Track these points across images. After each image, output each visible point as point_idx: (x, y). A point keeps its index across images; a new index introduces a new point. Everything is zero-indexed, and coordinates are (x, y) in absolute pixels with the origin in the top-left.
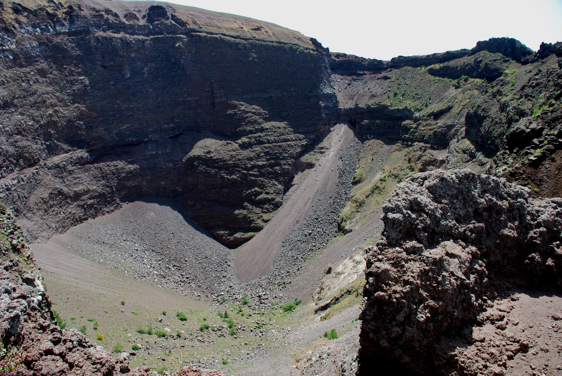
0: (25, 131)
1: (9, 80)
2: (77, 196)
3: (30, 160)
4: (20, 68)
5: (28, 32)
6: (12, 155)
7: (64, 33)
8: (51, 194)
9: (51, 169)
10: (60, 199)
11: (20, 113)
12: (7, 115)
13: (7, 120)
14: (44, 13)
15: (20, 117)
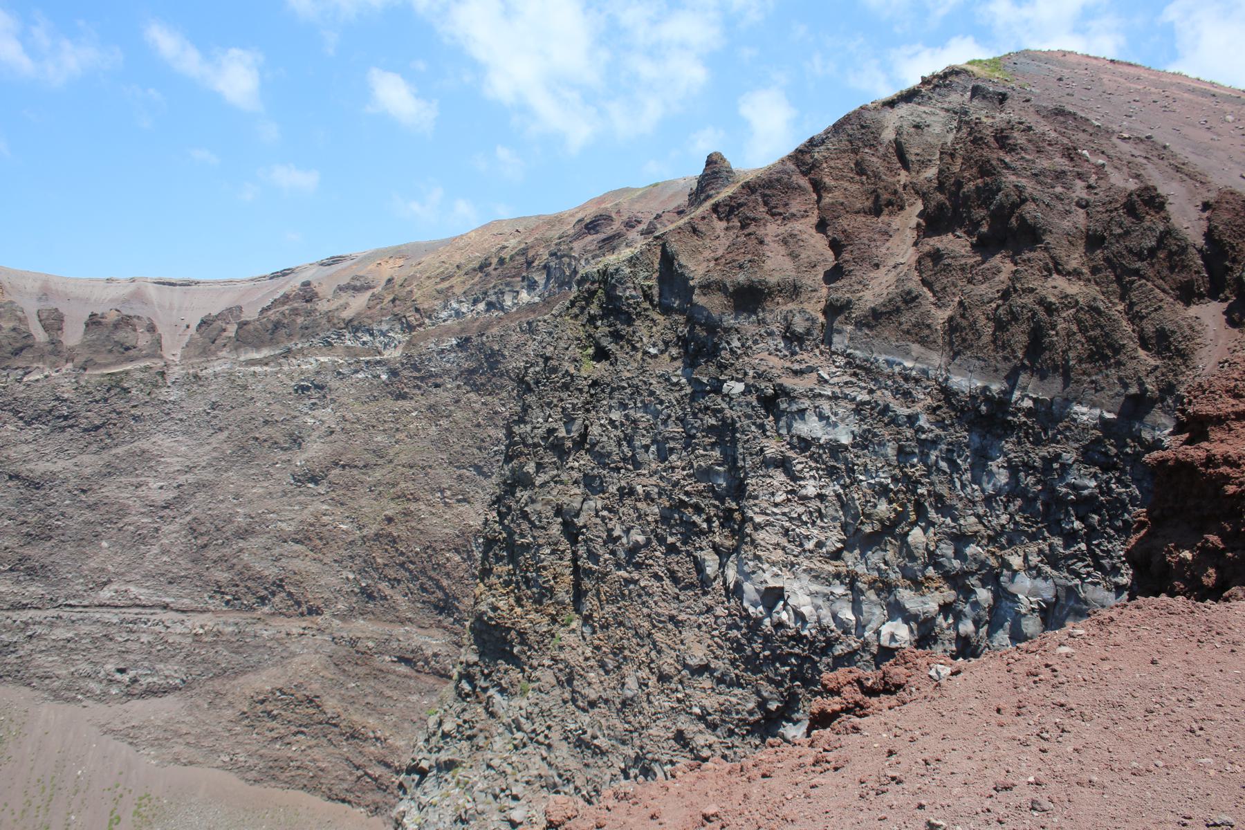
0: (321, 539)
1: (348, 426)
2: (353, 735)
3: (299, 604)
4: (397, 399)
5: (458, 314)
6: (259, 578)
7: (531, 307)
8: (280, 690)
9: (336, 643)
10: (310, 716)
11: (332, 499)
12: (302, 498)
13: (297, 508)
14: (522, 259)
15: (325, 507)
